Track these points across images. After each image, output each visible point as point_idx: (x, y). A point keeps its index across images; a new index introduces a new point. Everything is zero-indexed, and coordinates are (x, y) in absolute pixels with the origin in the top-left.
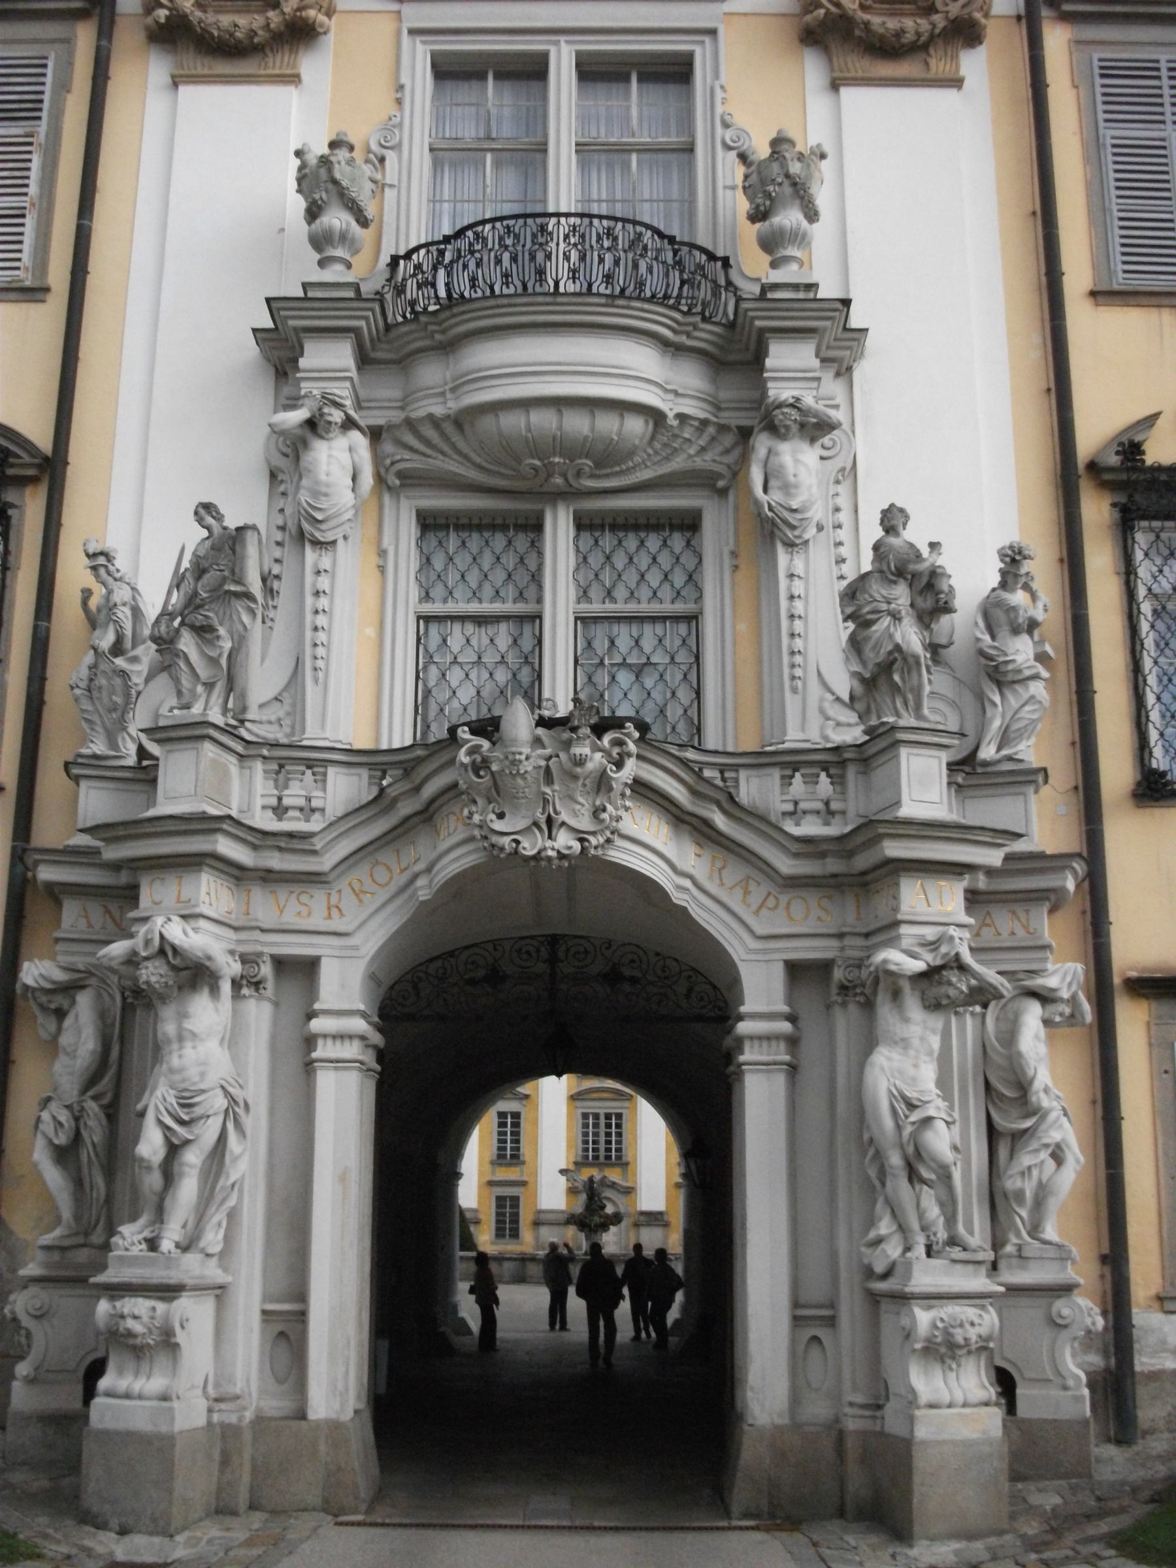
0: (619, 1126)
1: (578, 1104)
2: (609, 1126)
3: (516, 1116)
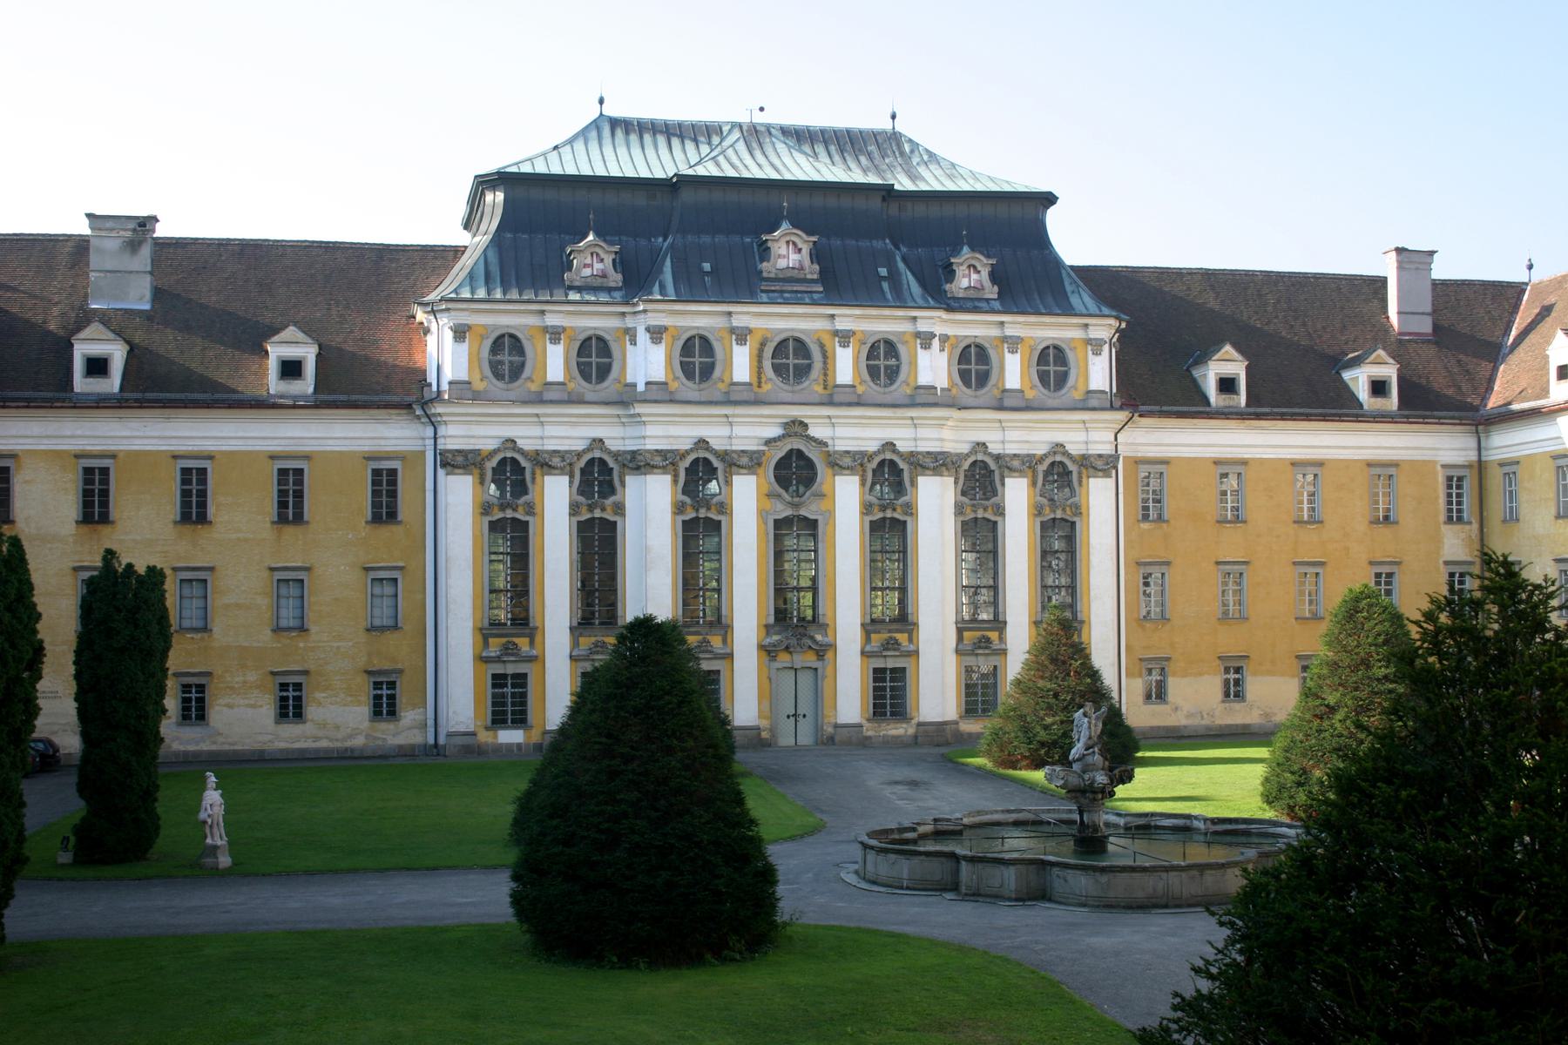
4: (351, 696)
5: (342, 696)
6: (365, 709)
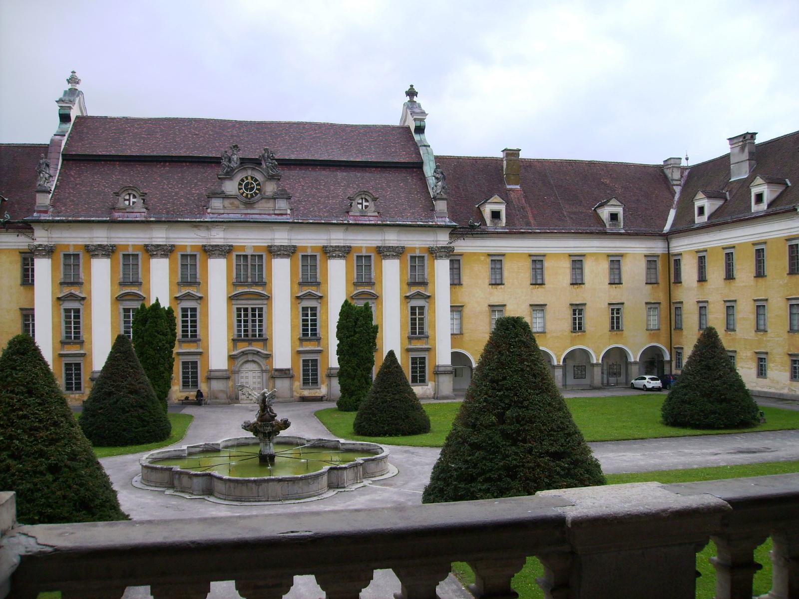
0: (260, 315)
1: (234, 302)
2: (254, 315)
3: (194, 310)
4: (783, 366)
5: (779, 366)
6: (787, 375)
